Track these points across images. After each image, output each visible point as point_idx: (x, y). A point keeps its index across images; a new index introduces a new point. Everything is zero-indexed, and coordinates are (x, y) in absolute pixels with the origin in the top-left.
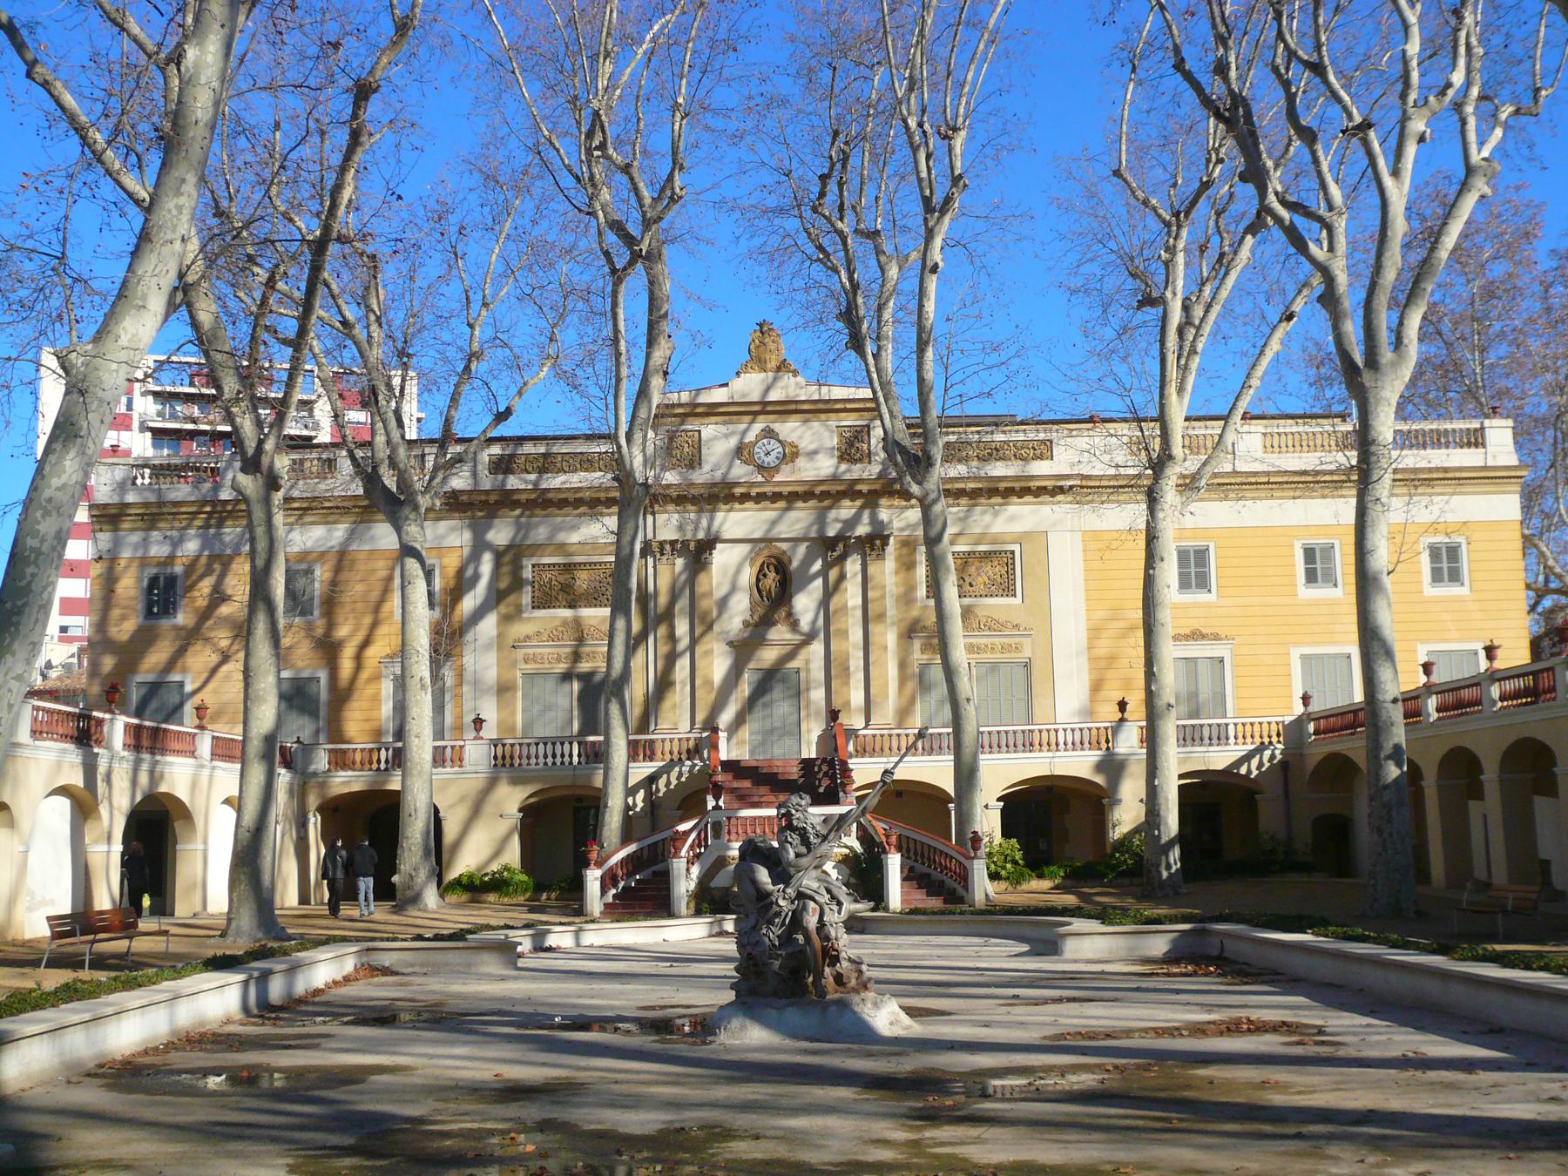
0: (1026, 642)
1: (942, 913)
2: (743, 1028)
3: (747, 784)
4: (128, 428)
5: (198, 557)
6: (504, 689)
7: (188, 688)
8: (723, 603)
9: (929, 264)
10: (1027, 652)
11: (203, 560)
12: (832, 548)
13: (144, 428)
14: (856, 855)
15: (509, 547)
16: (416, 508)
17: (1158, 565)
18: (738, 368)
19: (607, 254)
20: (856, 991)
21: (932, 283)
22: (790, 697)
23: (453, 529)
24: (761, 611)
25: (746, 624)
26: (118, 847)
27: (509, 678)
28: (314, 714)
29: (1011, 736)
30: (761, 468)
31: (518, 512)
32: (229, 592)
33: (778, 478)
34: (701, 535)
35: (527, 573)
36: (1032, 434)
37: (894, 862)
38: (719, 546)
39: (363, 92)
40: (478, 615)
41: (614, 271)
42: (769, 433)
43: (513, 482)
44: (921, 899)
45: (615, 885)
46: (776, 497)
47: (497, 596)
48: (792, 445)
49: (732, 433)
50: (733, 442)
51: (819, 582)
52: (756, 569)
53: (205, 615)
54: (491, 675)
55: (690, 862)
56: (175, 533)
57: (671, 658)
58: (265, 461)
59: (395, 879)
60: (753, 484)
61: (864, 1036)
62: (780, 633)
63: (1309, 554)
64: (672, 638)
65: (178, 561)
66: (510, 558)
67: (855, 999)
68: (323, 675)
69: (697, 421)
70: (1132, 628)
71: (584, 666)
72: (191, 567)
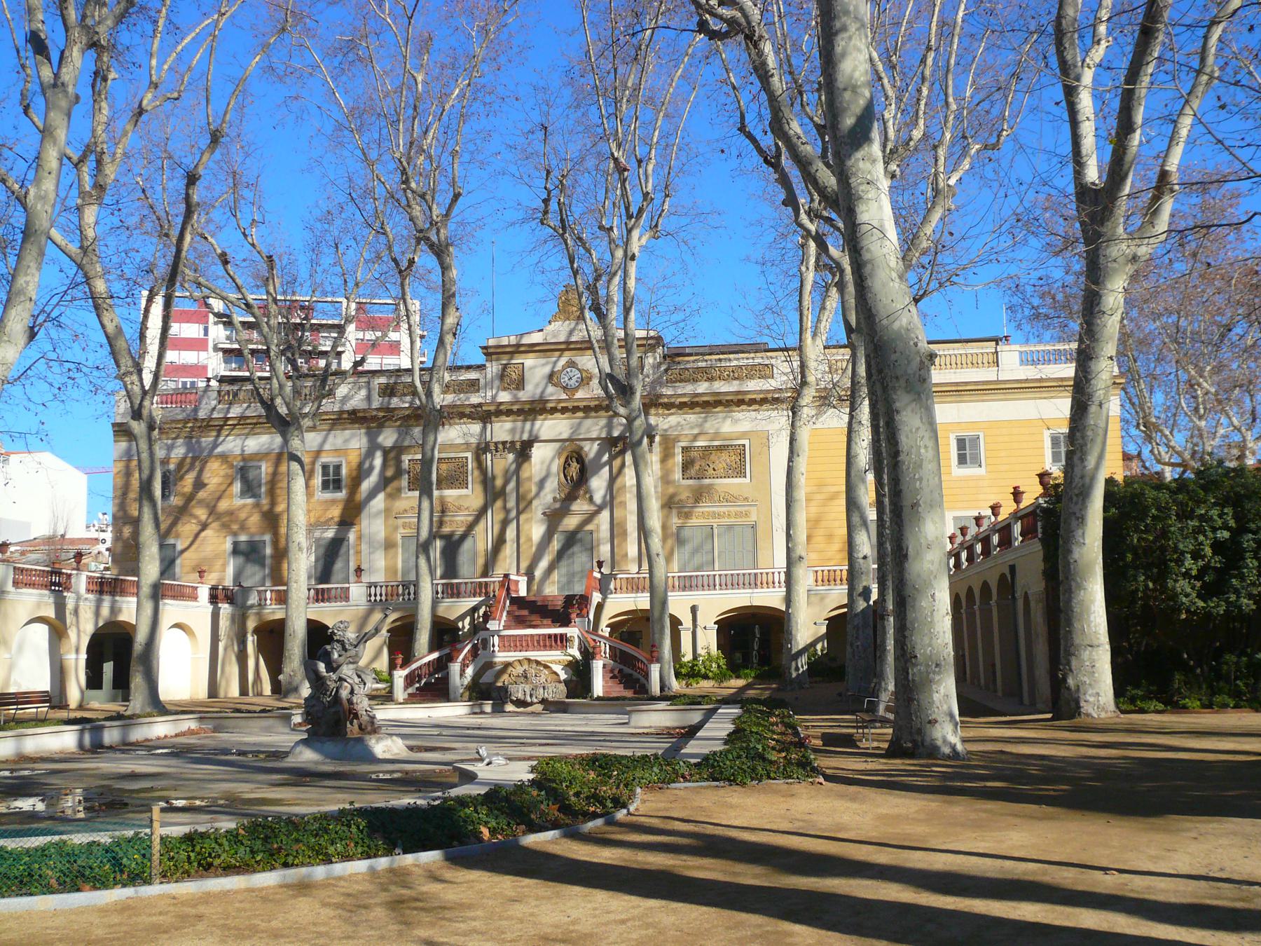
0: (754, 509)
1: (630, 699)
2: (301, 753)
3: (525, 612)
4: (206, 350)
5: (184, 459)
6: (389, 545)
7: (179, 547)
8: (541, 484)
9: (630, 254)
10: (754, 517)
11: (188, 460)
12: (617, 445)
13: (216, 349)
14: (577, 661)
15: (393, 448)
16: (299, 428)
17: (796, 459)
18: (549, 318)
19: (394, 260)
20: (370, 733)
21: (633, 268)
22: (586, 549)
23: (353, 436)
24: (567, 491)
25: (555, 499)
26: (83, 656)
27: (385, 539)
28: (263, 565)
29: (741, 578)
30: (565, 388)
31: (398, 423)
32: (206, 481)
33: (580, 394)
34: (525, 437)
35: (405, 465)
36: (759, 359)
37: (598, 666)
38: (536, 445)
39: (192, 179)
40: (372, 494)
41: (400, 272)
42: (571, 364)
43: (395, 402)
44: (618, 690)
45: (419, 682)
46: (575, 409)
47: (384, 482)
48: (587, 371)
49: (547, 363)
50: (547, 369)
51: (607, 468)
52: (563, 460)
53: (190, 498)
54: (382, 535)
55: (464, 666)
56: (170, 442)
57: (505, 523)
58: (145, 412)
59: (281, 677)
60: (560, 401)
61: (373, 760)
62: (580, 506)
63: (961, 443)
64: (507, 511)
65: (172, 461)
66: (393, 455)
67: (367, 737)
68: (267, 538)
69: (523, 355)
70: (833, 497)
71: (446, 530)
72: (180, 465)
